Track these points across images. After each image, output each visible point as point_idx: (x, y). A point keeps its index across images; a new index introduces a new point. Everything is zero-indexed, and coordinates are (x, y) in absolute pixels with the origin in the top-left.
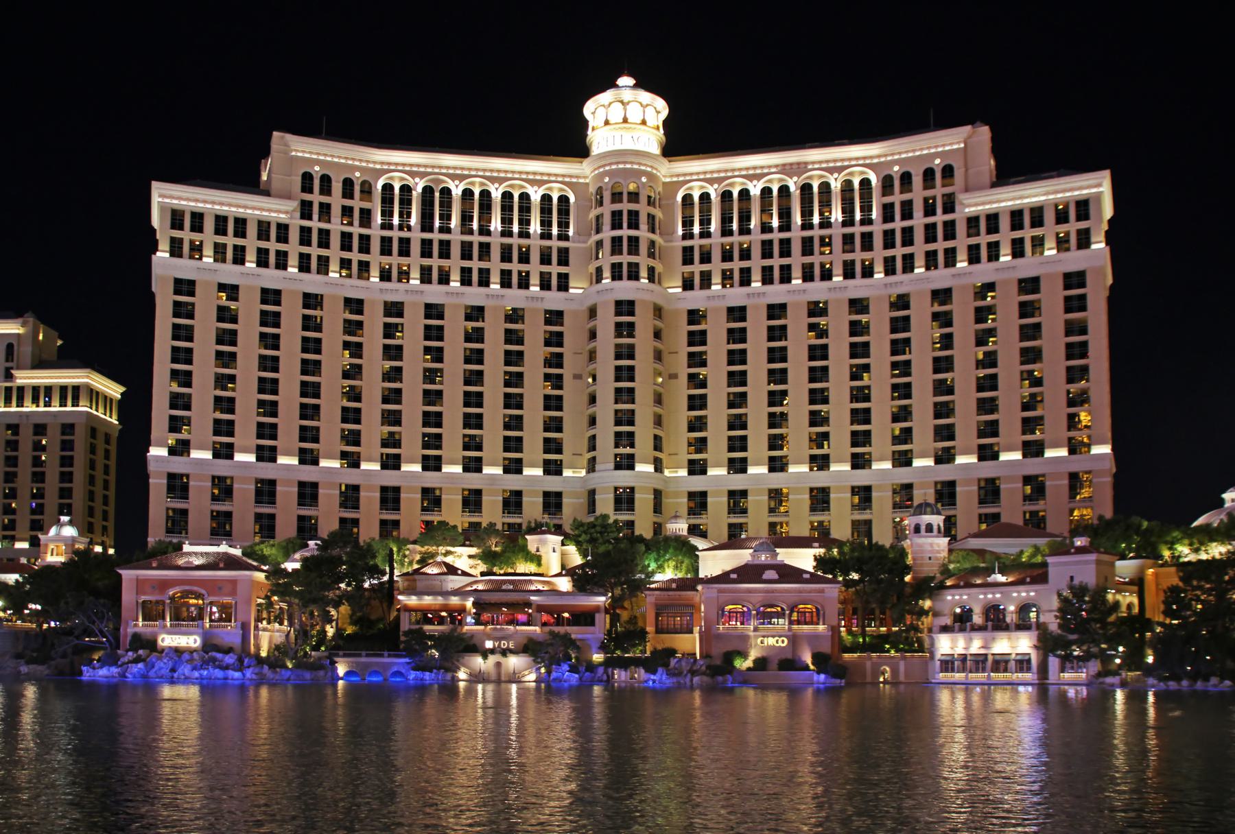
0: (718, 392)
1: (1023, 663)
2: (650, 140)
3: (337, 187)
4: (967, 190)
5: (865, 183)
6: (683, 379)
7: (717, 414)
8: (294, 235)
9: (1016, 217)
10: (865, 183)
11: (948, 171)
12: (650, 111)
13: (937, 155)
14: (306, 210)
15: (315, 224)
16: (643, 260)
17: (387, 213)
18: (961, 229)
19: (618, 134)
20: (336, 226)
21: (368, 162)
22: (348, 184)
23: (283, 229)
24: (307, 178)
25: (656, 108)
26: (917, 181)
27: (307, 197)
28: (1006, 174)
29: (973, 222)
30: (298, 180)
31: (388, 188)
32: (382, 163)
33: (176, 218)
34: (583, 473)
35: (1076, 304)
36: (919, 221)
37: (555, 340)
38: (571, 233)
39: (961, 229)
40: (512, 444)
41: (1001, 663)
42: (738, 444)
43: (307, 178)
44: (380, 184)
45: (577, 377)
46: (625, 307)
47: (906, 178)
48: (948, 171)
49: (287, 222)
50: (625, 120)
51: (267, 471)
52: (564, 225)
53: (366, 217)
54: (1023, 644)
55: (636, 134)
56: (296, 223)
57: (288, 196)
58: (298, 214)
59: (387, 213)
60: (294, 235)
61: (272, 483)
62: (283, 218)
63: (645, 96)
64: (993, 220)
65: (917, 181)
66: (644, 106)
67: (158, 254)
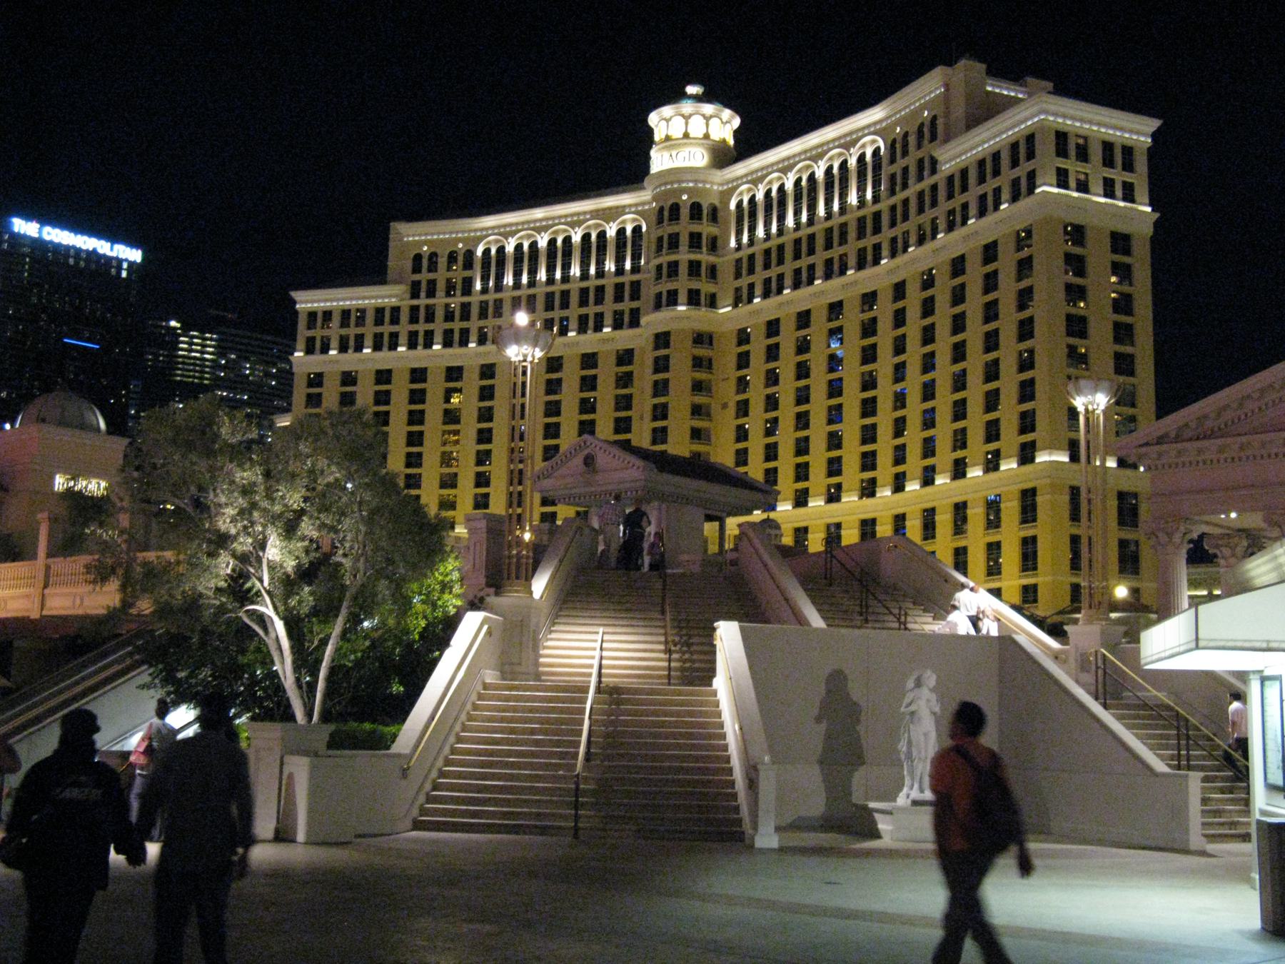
3: (442, 261)
8: (404, 316)
15: (423, 301)
17: (485, 279)
20: (440, 300)
21: (470, 231)
23: (396, 310)
24: (418, 258)
27: (417, 277)
30: (409, 265)
33: (312, 315)
43: (418, 258)
44: (479, 252)
49: (398, 304)
50: (687, 133)
58: (408, 296)
60: (404, 316)
62: (394, 301)
67: (296, 354)
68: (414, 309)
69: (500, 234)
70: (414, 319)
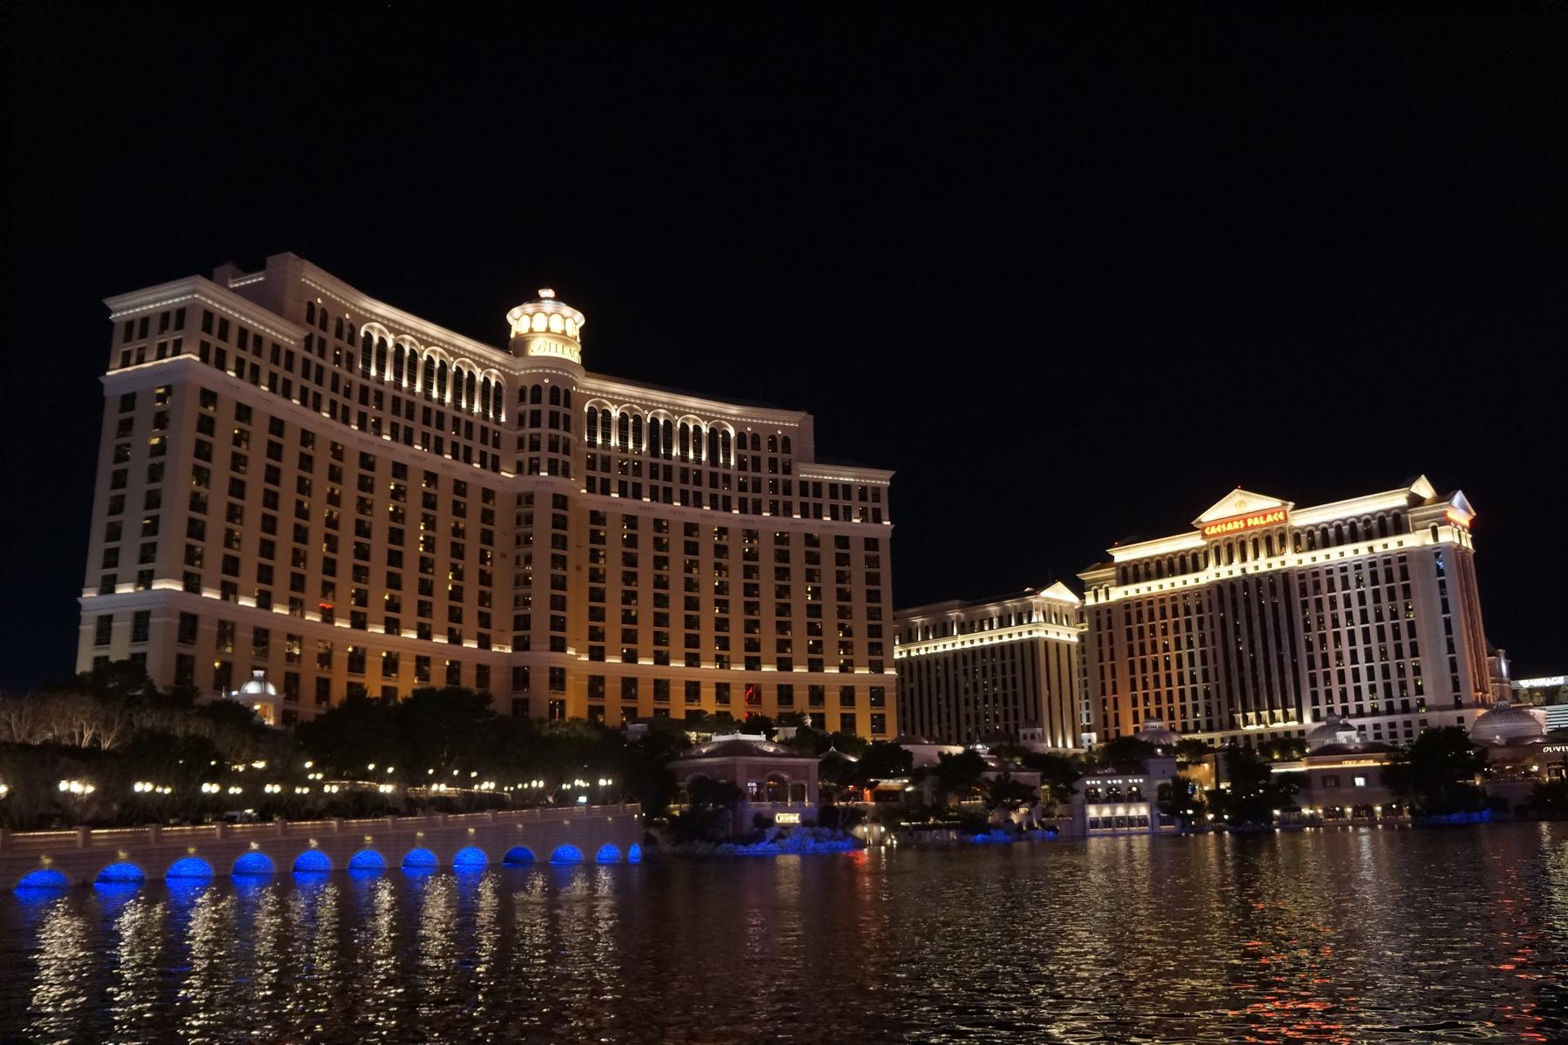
0: (614, 588)
1: (1142, 821)
2: (573, 354)
4: (802, 460)
6: (586, 574)
7: (613, 608)
8: (298, 366)
9: (833, 487)
11: (786, 441)
12: (569, 321)
13: (780, 427)
14: (308, 341)
18: (796, 490)
19: (554, 343)
22: (340, 322)
23: (290, 354)
25: (572, 321)
28: (826, 453)
29: (804, 484)
31: (369, 336)
32: (366, 310)
34: (508, 650)
35: (872, 562)
37: (487, 516)
38: (503, 419)
39: (796, 490)
40: (659, 639)
41: (1130, 821)
42: (692, 641)
43: (311, 306)
45: (504, 556)
46: (560, 501)
47: (755, 437)
48: (786, 441)
51: (785, 678)
52: (497, 412)
54: (1142, 810)
56: (301, 353)
57: (296, 322)
61: (790, 687)
63: (567, 310)
64: (818, 485)
65: (764, 443)
66: (565, 318)
69: (387, 326)
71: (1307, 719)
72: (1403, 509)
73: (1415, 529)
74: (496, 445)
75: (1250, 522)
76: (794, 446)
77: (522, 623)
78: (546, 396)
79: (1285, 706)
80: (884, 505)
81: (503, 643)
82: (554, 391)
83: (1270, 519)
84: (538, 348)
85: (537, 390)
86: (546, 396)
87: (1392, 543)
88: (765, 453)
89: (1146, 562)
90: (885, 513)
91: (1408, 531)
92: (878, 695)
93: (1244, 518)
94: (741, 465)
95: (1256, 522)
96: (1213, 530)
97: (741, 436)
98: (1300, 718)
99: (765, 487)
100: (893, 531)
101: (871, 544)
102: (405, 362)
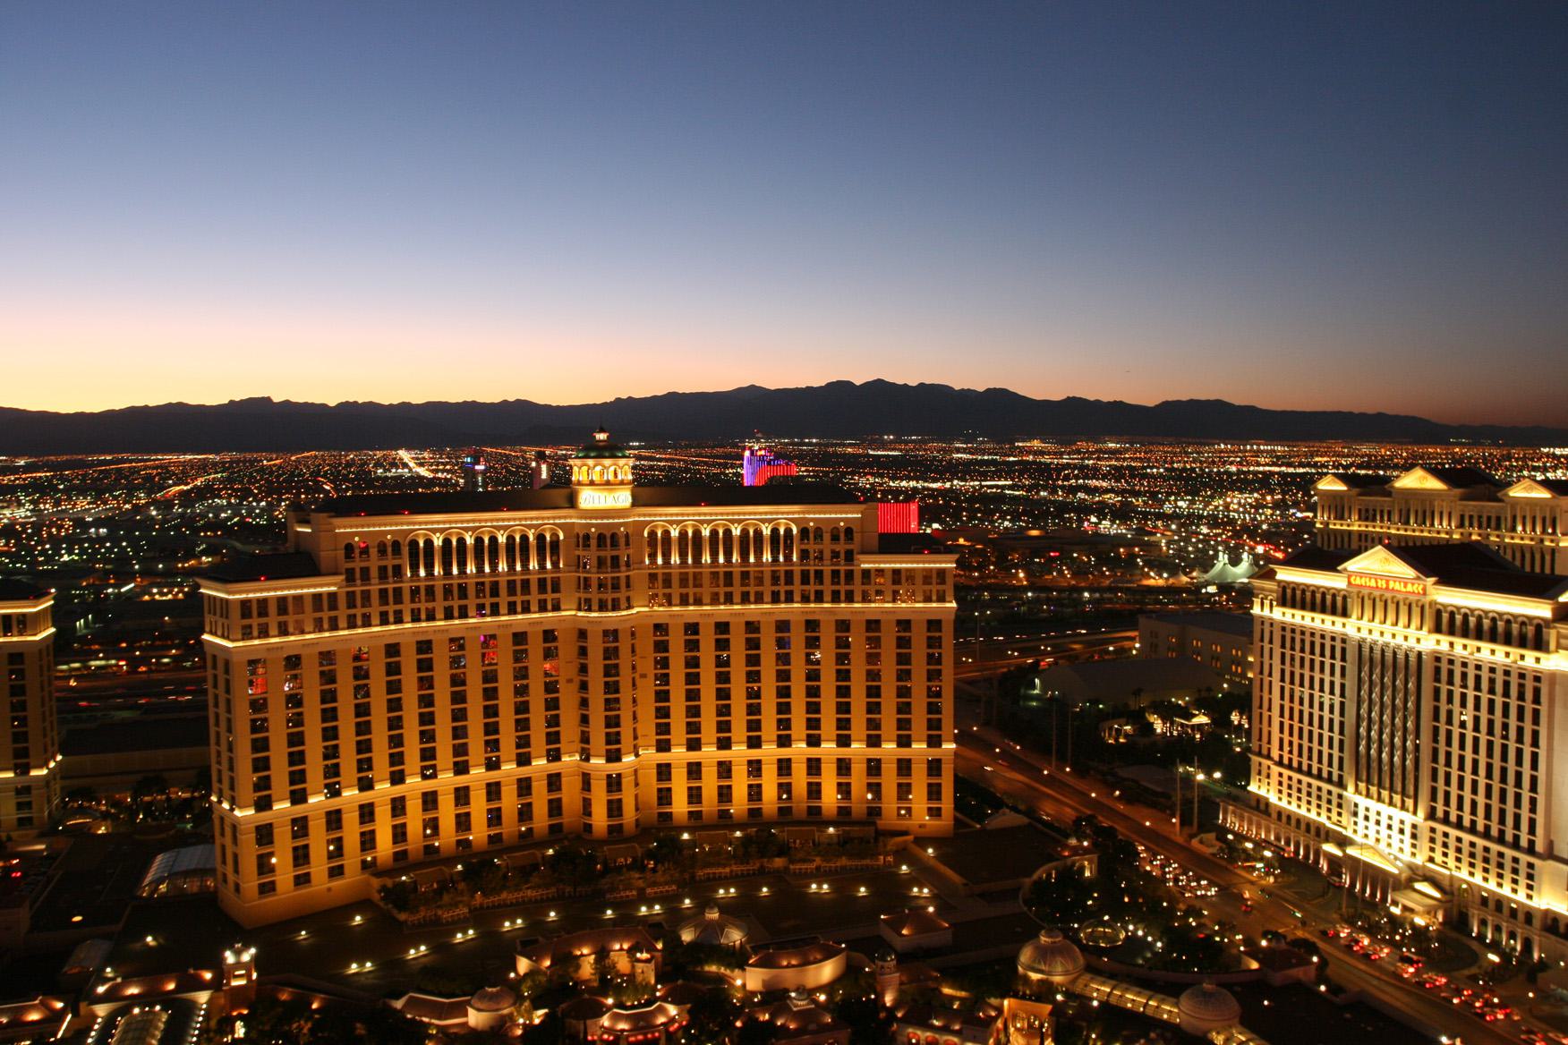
4: (863, 552)
5: (789, 531)
8: (342, 602)
10: (789, 531)
14: (350, 577)
16: (622, 595)
18: (858, 577)
26: (827, 537)
29: (866, 573)
36: (827, 569)
43: (349, 548)
45: (570, 681)
47: (818, 533)
48: (849, 532)
53: (398, 570)
55: (617, 494)
59: (415, 568)
60: (342, 602)
62: (333, 589)
68: (351, 595)
70: (351, 605)
71: (1421, 813)
72: (1547, 623)
73: (1559, 646)
74: (556, 589)
75: (1391, 585)
76: (857, 537)
77: (585, 739)
78: (593, 542)
79: (1404, 794)
80: (949, 589)
81: (571, 753)
82: (601, 537)
83: (1410, 588)
84: (589, 499)
85: (587, 537)
86: (593, 542)
87: (1529, 659)
88: (827, 546)
89: (1305, 588)
90: (950, 593)
91: (1547, 651)
92: (934, 767)
93: (1388, 579)
94: (804, 555)
95: (1398, 586)
96: (1358, 581)
97: (804, 532)
98: (1415, 813)
99: (827, 578)
100: (959, 609)
101: (934, 625)
102: (453, 552)
